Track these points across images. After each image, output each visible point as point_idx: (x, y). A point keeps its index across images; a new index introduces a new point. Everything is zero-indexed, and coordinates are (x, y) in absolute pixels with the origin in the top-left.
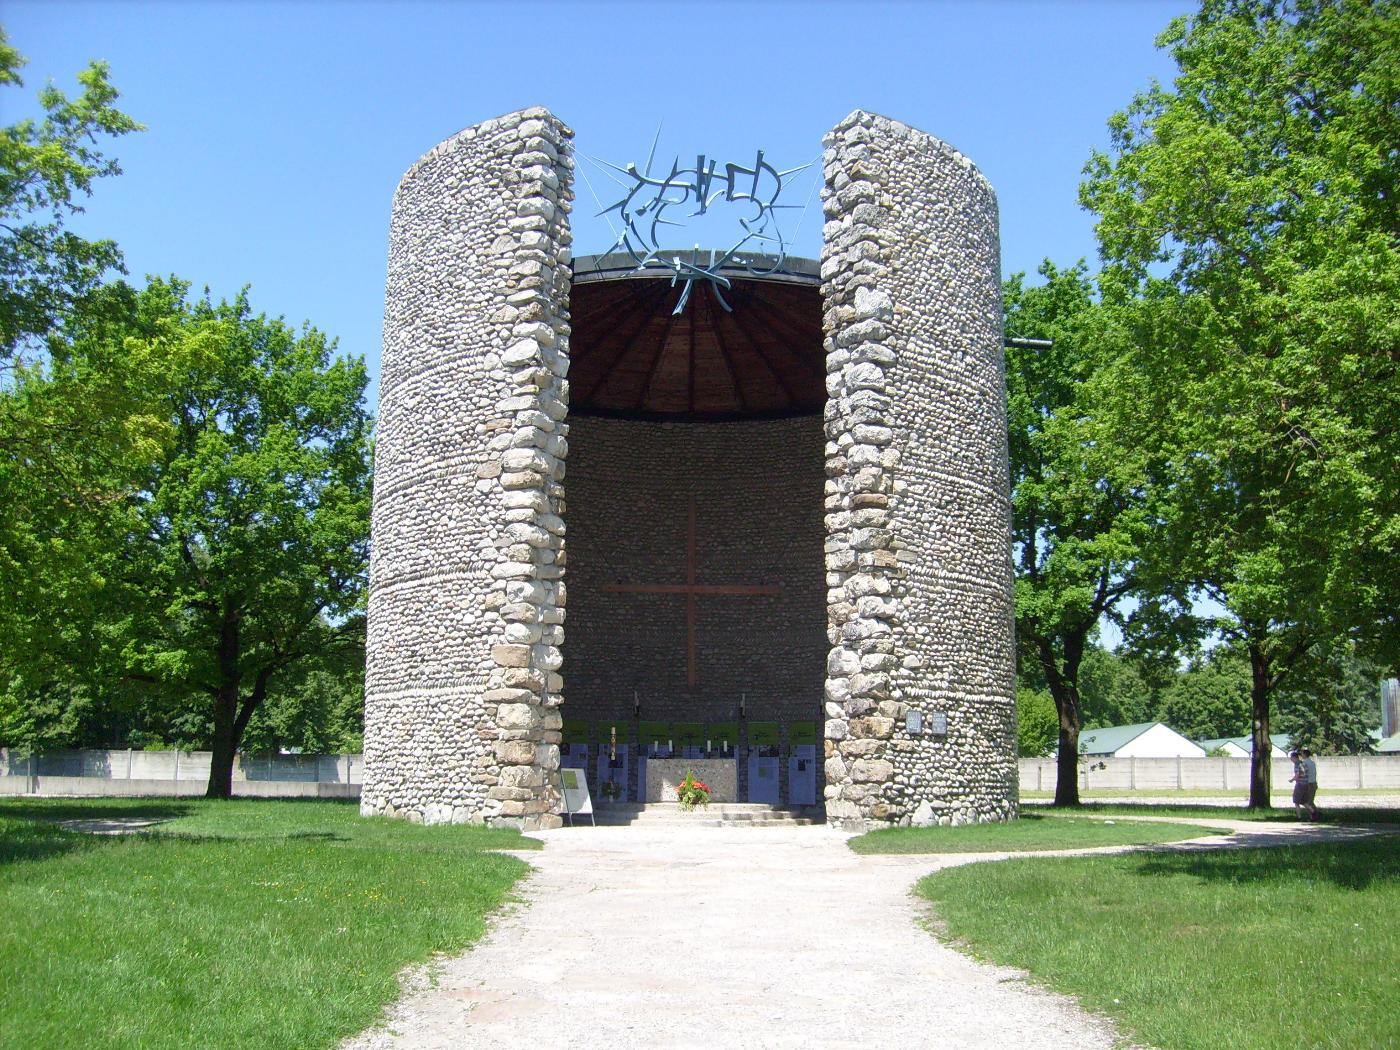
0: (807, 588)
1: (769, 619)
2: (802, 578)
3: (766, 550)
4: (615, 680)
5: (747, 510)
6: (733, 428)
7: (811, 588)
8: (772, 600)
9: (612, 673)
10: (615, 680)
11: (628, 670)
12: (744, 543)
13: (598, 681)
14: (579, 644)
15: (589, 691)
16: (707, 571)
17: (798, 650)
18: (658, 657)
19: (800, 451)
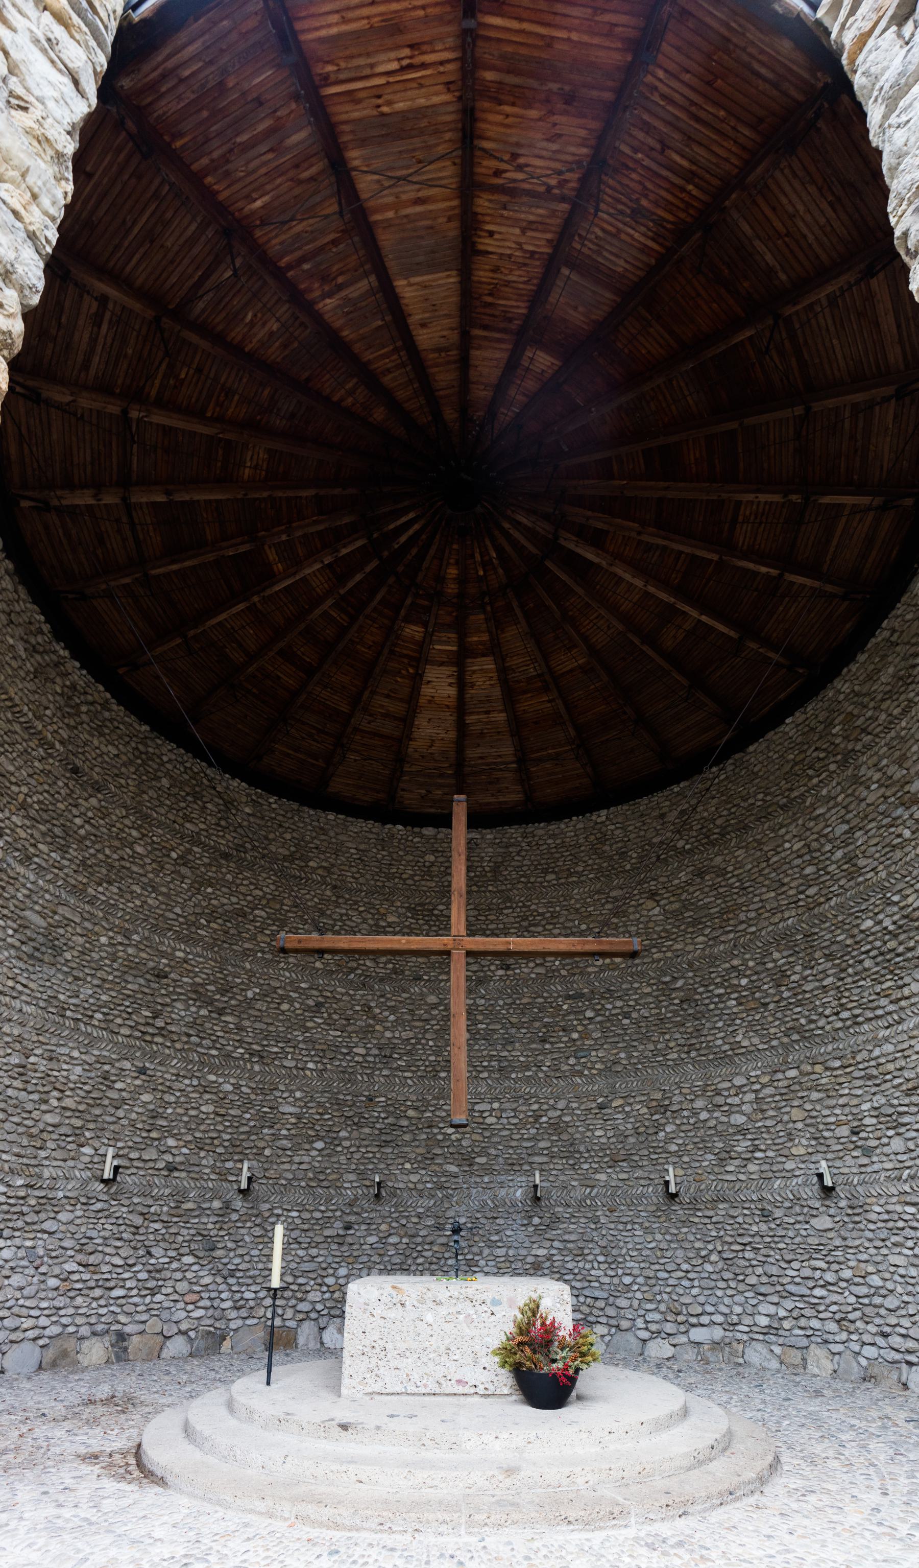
0: (627, 1015)
1: (572, 1061)
2: (619, 1004)
3: (564, 972)
4: (346, 1143)
5: (535, 925)
6: (514, 832)
7: (634, 1015)
8: (575, 1036)
9: (343, 1134)
10: (346, 1143)
11: (367, 1130)
12: (531, 965)
13: (319, 1145)
14: (292, 1092)
15: (306, 1159)
16: (483, 1001)
17: (620, 1102)
18: (411, 1113)
19: (607, 848)
